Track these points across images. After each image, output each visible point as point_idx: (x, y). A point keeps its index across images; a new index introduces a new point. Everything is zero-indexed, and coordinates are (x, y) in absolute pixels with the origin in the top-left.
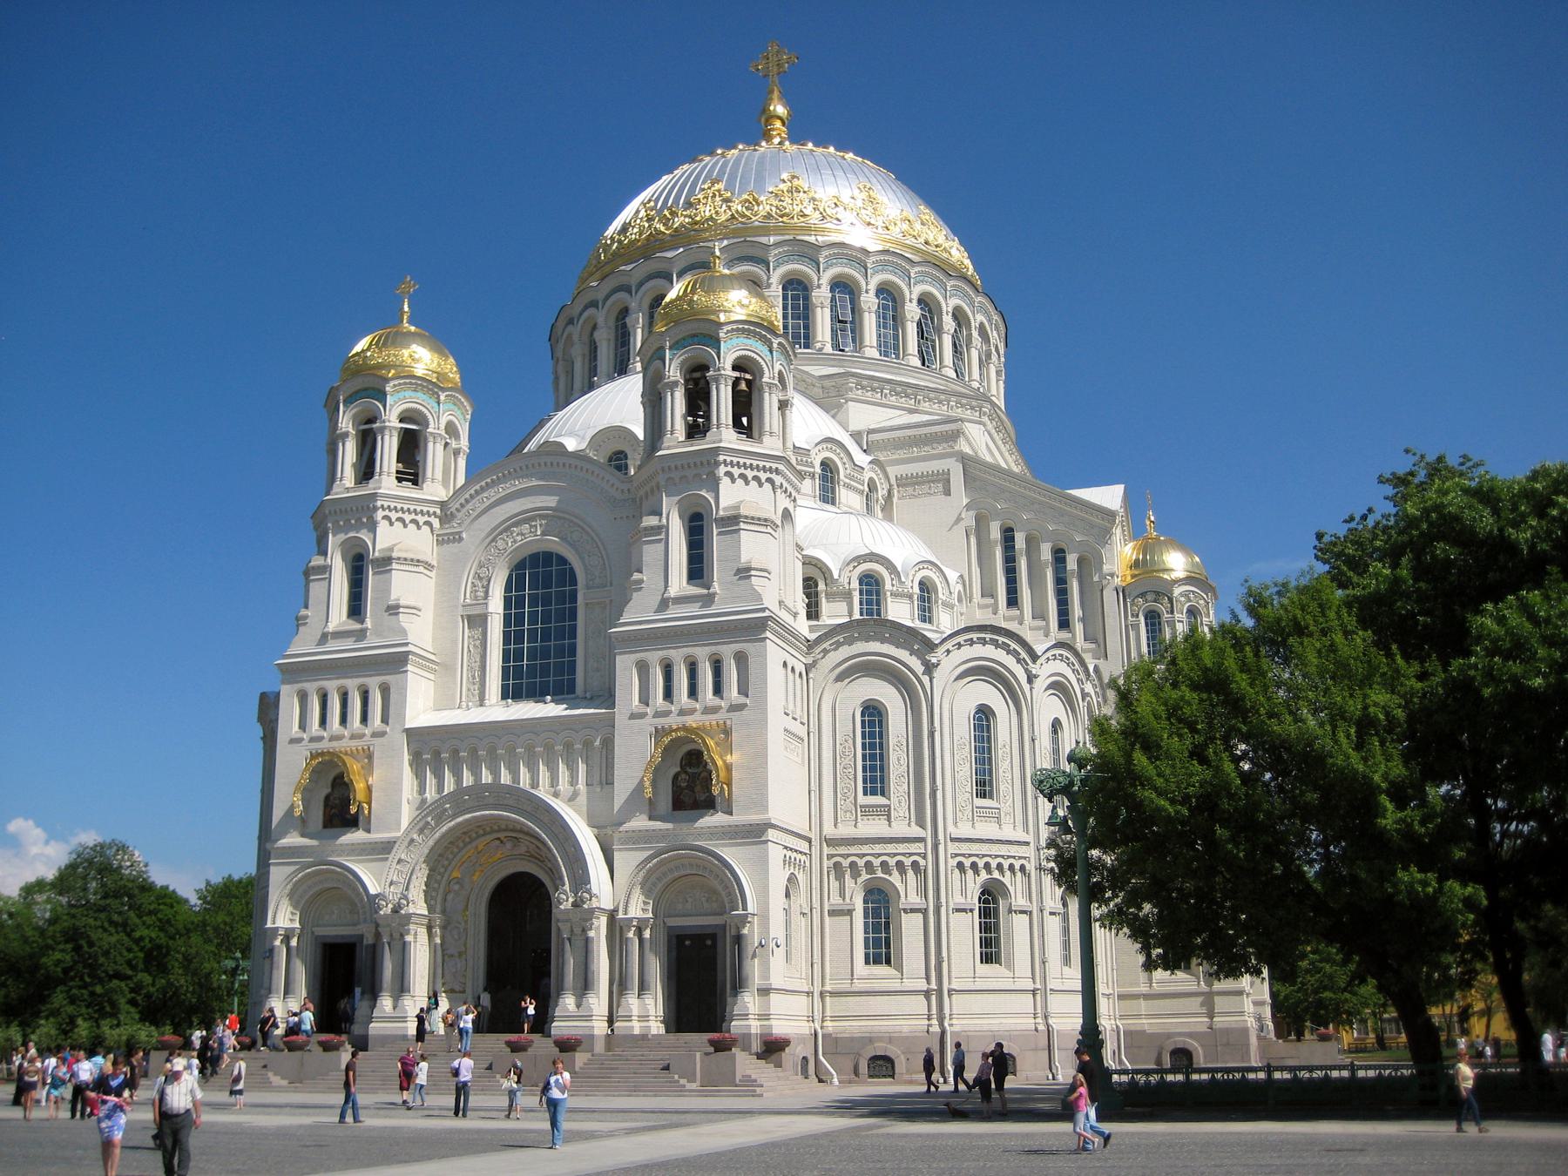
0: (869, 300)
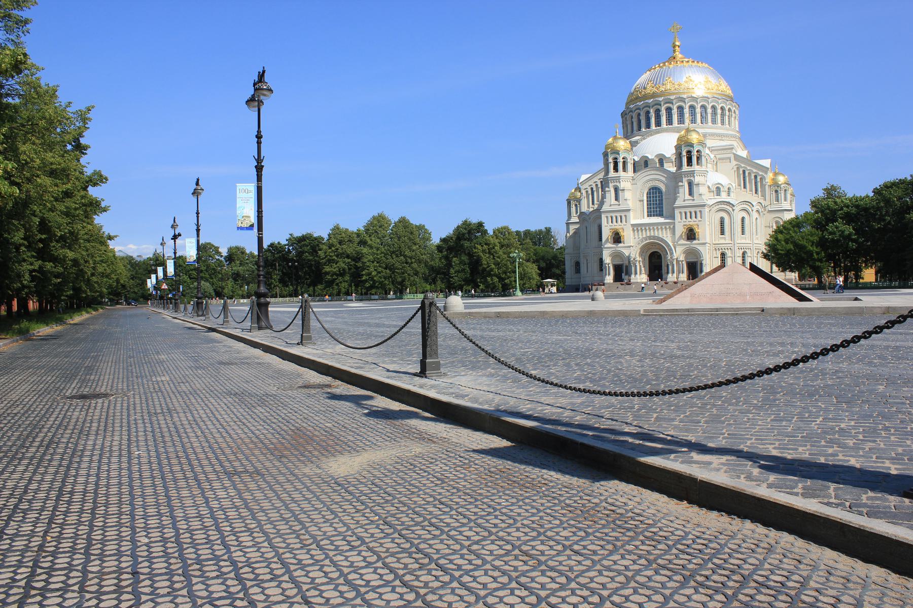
0: (709, 111)
